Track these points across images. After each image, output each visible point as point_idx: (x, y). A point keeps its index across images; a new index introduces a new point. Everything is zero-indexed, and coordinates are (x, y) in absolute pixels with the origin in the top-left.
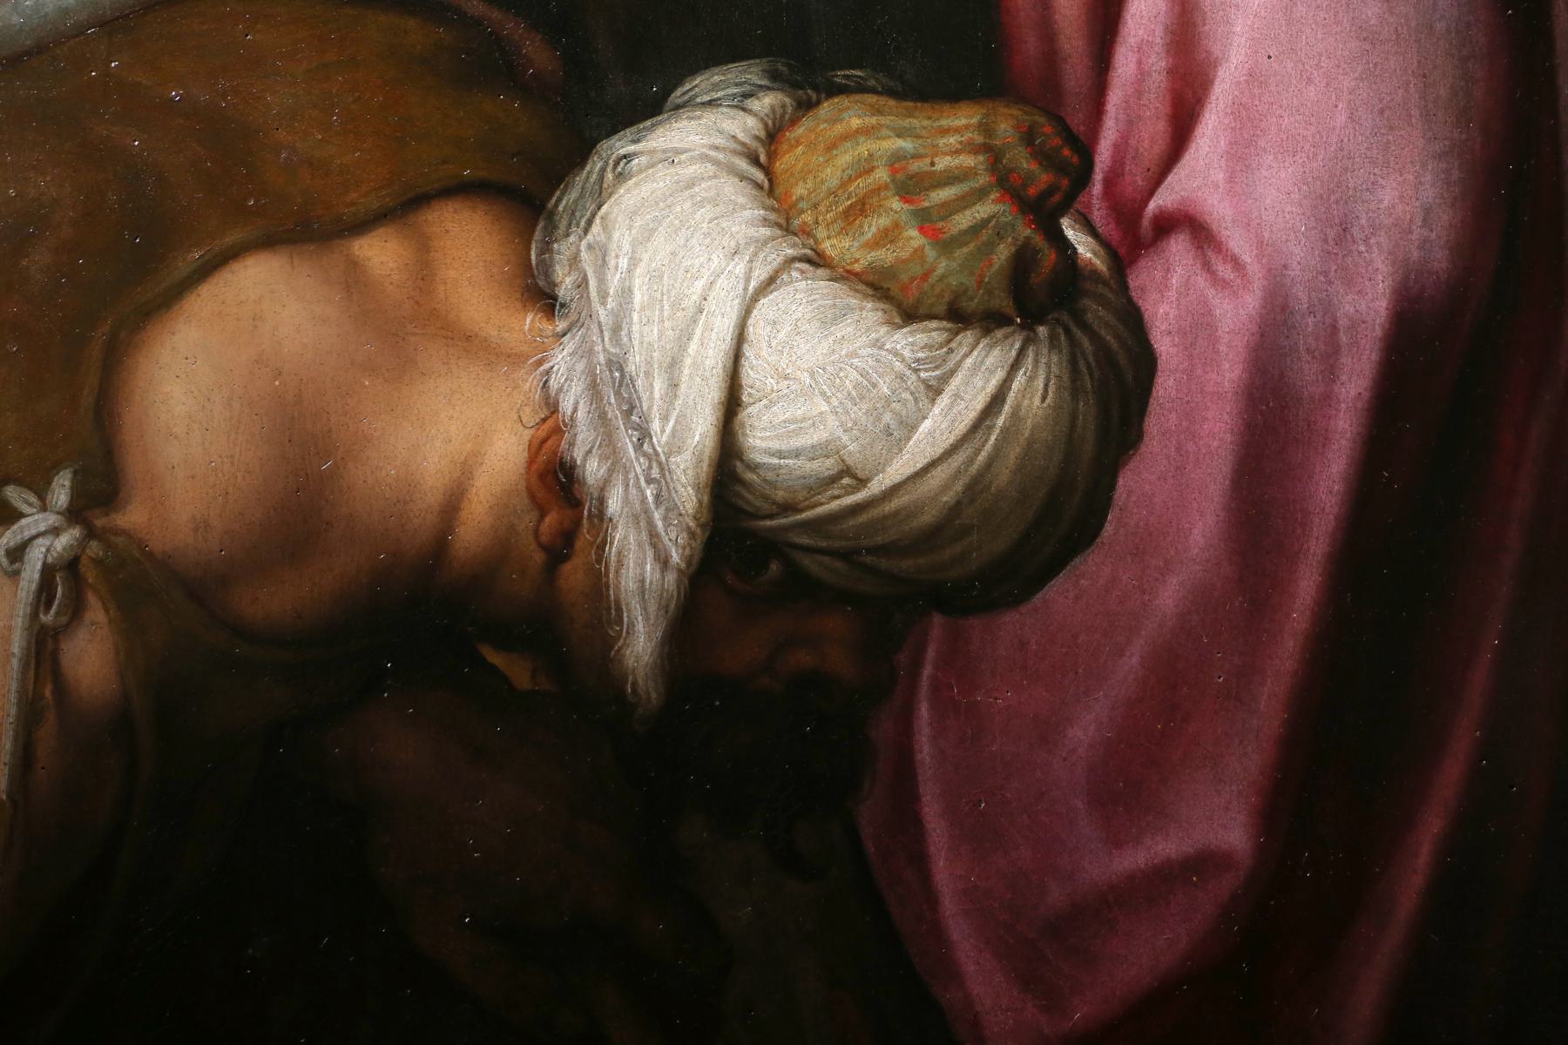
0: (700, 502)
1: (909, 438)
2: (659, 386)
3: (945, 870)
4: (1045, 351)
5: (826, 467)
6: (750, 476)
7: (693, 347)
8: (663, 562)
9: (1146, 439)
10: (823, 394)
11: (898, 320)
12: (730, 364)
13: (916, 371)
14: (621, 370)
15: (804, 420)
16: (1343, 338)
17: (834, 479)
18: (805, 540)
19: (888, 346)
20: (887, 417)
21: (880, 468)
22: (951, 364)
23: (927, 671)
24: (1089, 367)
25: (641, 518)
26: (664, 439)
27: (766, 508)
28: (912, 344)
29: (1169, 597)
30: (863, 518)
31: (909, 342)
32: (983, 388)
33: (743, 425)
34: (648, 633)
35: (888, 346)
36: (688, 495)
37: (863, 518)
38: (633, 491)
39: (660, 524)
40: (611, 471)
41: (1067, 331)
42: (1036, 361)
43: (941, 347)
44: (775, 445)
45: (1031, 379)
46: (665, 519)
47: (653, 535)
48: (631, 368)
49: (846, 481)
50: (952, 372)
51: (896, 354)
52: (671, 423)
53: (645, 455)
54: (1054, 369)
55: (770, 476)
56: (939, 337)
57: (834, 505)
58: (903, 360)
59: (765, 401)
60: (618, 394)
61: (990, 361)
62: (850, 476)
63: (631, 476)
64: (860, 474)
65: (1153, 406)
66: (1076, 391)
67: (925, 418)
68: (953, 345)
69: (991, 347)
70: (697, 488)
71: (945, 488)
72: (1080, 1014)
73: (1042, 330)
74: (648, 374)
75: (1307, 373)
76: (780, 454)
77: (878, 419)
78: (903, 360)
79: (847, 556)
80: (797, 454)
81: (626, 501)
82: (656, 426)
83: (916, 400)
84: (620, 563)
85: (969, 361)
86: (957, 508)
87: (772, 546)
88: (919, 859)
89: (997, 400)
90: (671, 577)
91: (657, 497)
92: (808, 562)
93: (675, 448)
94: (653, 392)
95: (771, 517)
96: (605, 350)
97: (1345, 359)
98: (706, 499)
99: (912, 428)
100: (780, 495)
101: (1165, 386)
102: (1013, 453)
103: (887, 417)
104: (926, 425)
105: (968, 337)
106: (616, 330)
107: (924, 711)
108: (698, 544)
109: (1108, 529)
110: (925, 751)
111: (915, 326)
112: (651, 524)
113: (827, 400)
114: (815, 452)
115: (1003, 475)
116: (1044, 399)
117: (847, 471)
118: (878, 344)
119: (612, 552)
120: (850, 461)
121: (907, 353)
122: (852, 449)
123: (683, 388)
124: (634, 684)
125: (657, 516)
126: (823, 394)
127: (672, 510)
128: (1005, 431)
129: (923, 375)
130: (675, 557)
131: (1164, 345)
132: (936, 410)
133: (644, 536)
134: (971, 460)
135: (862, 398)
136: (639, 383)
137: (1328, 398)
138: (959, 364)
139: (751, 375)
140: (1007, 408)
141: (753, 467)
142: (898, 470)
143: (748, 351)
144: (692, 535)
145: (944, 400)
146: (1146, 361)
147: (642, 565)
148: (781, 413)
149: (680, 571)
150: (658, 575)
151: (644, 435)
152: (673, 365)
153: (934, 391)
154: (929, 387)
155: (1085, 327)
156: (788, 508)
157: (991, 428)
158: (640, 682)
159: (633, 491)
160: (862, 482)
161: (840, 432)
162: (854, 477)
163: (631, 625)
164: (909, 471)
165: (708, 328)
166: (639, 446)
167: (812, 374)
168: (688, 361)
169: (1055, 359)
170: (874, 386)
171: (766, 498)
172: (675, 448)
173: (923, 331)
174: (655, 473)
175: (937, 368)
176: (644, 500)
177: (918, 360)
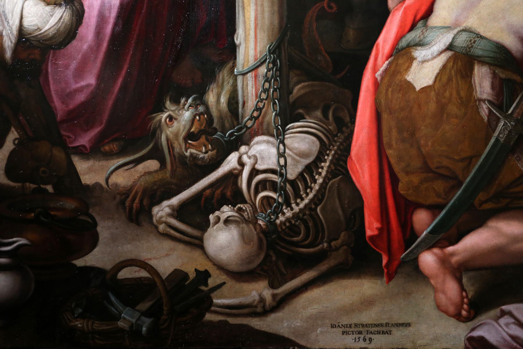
0: (17, 33)
1: (48, 23)
2: (10, 15)
3: (52, 87)
4: (68, 10)
5: (36, 28)
6: (24, 29)
7: (15, 9)
8: (12, 42)
9: (83, 23)
10: (35, 16)
11: (47, 5)
12: (21, 12)
13: (49, 13)
14: (5, 12)
15: (32, 20)
16: (112, 7)
17: (37, 30)
18: (33, 39)
19: (45, 9)
20: (45, 20)
21: (44, 28)
22: (54, 12)
23: (50, 58)
24: (75, 12)
25: (8, 35)
26: (11, 23)
27: (27, 34)
28: (49, 9)
29: (85, 47)
30: (42, 35)
31: (48, 8)
32: (59, 16)
33: (23, 21)
34: (10, 53)
35: (45, 9)
36: (15, 32)
37: (42, 35)
38: (7, 31)
39: (11, 36)
40: (4, 28)
41: (72, 7)
42: (67, 12)
43: (53, 9)
44: (28, 24)
45: (66, 14)
46: (12, 36)
47: (10, 39)
48: (6, 12)
49: (39, 30)
50: (55, 13)
51: (46, 10)
52: (12, 21)
53: (8, 26)
54: (70, 13)
55: (27, 29)
56: (53, 8)
57: (37, 34)
58: (47, 11)
59: (26, 18)
60: (4, 16)
61: (60, 11)
62: (39, 29)
63: (6, 29)
64: (41, 29)
65: (84, 18)
66: (73, 16)
67: (50, 20)
68: (55, 9)
69: (60, 9)
70: (17, 31)
71: (53, 31)
72: (71, 107)
73: (68, 7)
74: (9, 13)
75: (107, 13)
76: (29, 26)
77: (43, 20)
78: (47, 11)
79: (39, 41)
80: (31, 26)
81: (6, 33)
82: (10, 21)
83: (49, 17)
84: (5, 42)
85: (57, 11)
86: (55, 34)
87: (27, 40)
88: (49, 85)
89: (61, 17)
90: (13, 45)
91: (11, 33)
92: (33, 42)
93: (13, 25)
94: (9, 16)
95: (28, 35)
96: (2, 10)
97: (112, 10)
98: (18, 33)
99: (48, 21)
100: (29, 32)
101: (86, 15)
102: (63, 25)
103: (45, 20)
104: (50, 21)
105: (57, 8)
106: (4, 6)
107: (50, 64)
108: (17, 39)
109: (77, 37)
110: (50, 70)
111: (49, 6)
112: (10, 37)
113: (36, 17)
114: (34, 25)
115: (62, 29)
116: (68, 17)
117: (39, 28)
118: (43, 9)
119: (4, 40)
120: (39, 27)
121: (48, 10)
122: (40, 25)
123: (14, 16)
124: (8, 60)
125: (10, 35)
126: (35, 16)
127: (13, 34)
128: (62, 22)
129: (50, 13)
130: (13, 41)
131: (86, 9)
132: (52, 19)
133: (9, 38)
134: (57, 26)
135: (41, 17)
136: (7, 15)
137: (110, 17)
138: (56, 12)
139: (24, 13)
140: (63, 19)
141: (25, 28)
142: (46, 28)
143: (24, 10)
144: (16, 38)
145: (53, 17)
146: (83, 11)
147: (8, 42)
148: (29, 19)
149: (14, 44)
150: (11, 44)
151: (8, 23)
152: (12, 12)
153: (52, 16)
154: (51, 15)
155: (74, 6)
156: (30, 34)
157: (60, 22)
158: (8, 60)
159: (7, 31)
160: (41, 30)
161: (38, 22)
162: (40, 29)
163: (7, 52)
164: (48, 28)
165: (18, 6)
166: (8, 25)
167: (34, 13)
168: (15, 11)
169: (70, 11)
170: (43, 15)
171: (27, 32)
172: (13, 25)
173: (50, 7)
174: (10, 29)
175: (52, 12)
176: (8, 33)
177: (49, 11)
